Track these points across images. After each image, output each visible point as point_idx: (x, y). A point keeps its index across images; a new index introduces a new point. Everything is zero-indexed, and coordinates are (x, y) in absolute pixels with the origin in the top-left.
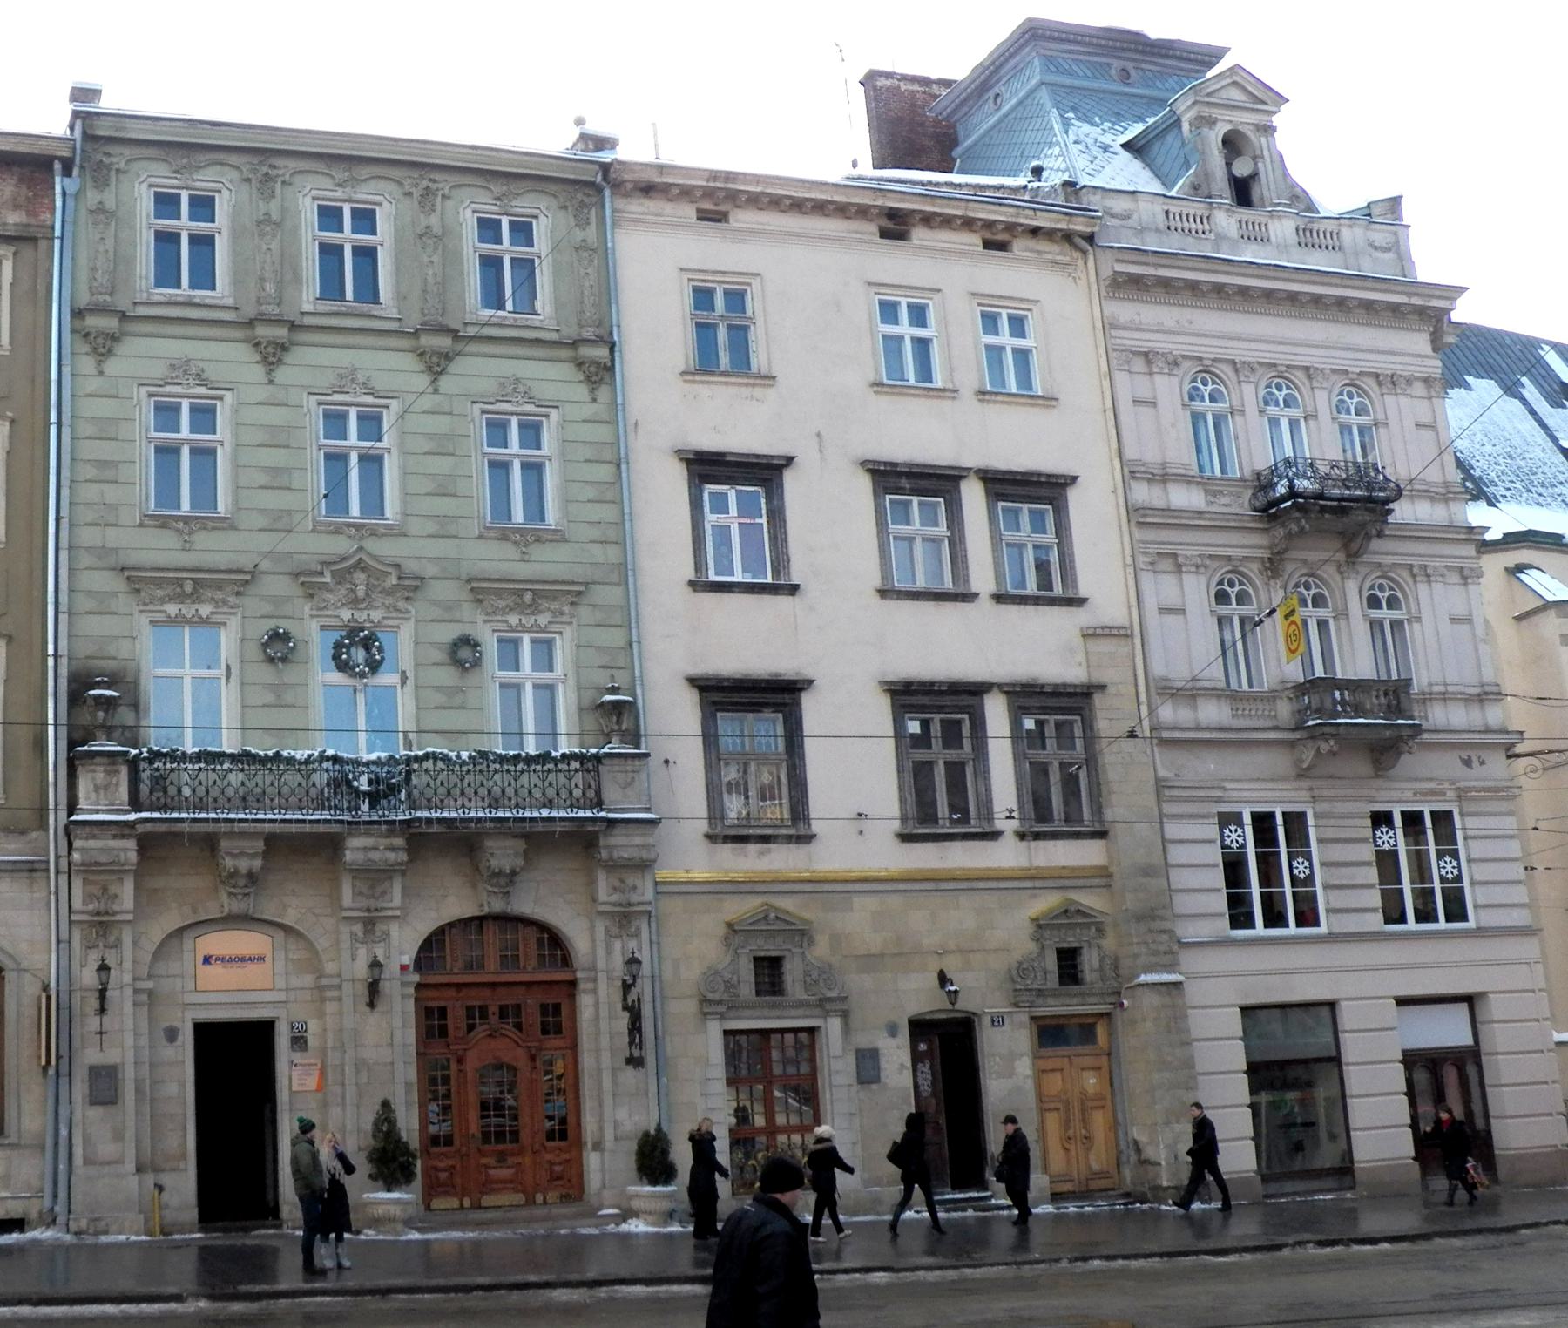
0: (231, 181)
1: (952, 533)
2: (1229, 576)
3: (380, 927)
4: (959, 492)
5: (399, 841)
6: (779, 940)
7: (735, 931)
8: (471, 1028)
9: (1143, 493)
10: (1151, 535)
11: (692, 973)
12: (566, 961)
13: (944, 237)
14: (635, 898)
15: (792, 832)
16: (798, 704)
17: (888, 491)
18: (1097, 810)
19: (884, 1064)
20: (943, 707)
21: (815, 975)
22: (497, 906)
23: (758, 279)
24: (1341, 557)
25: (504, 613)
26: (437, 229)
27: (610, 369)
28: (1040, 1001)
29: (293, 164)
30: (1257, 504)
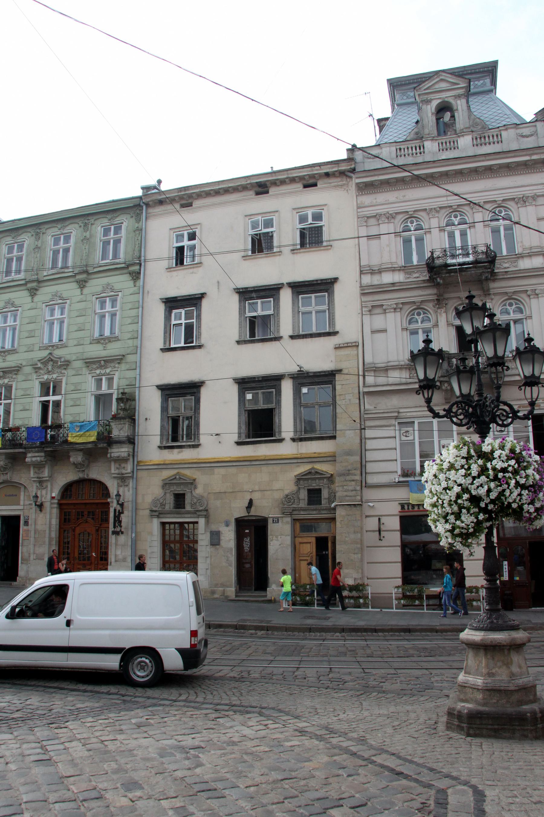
0: (28, 237)
2: (417, 311)
3: (44, 485)
4: (279, 294)
5: (42, 454)
8: (78, 519)
10: (370, 298)
11: (149, 499)
14: (124, 471)
16: (199, 392)
17: (246, 299)
19: (222, 538)
21: (195, 500)
22: (81, 475)
23: (200, 225)
25: (96, 370)
26: (88, 237)
28: (295, 512)
29: (47, 226)
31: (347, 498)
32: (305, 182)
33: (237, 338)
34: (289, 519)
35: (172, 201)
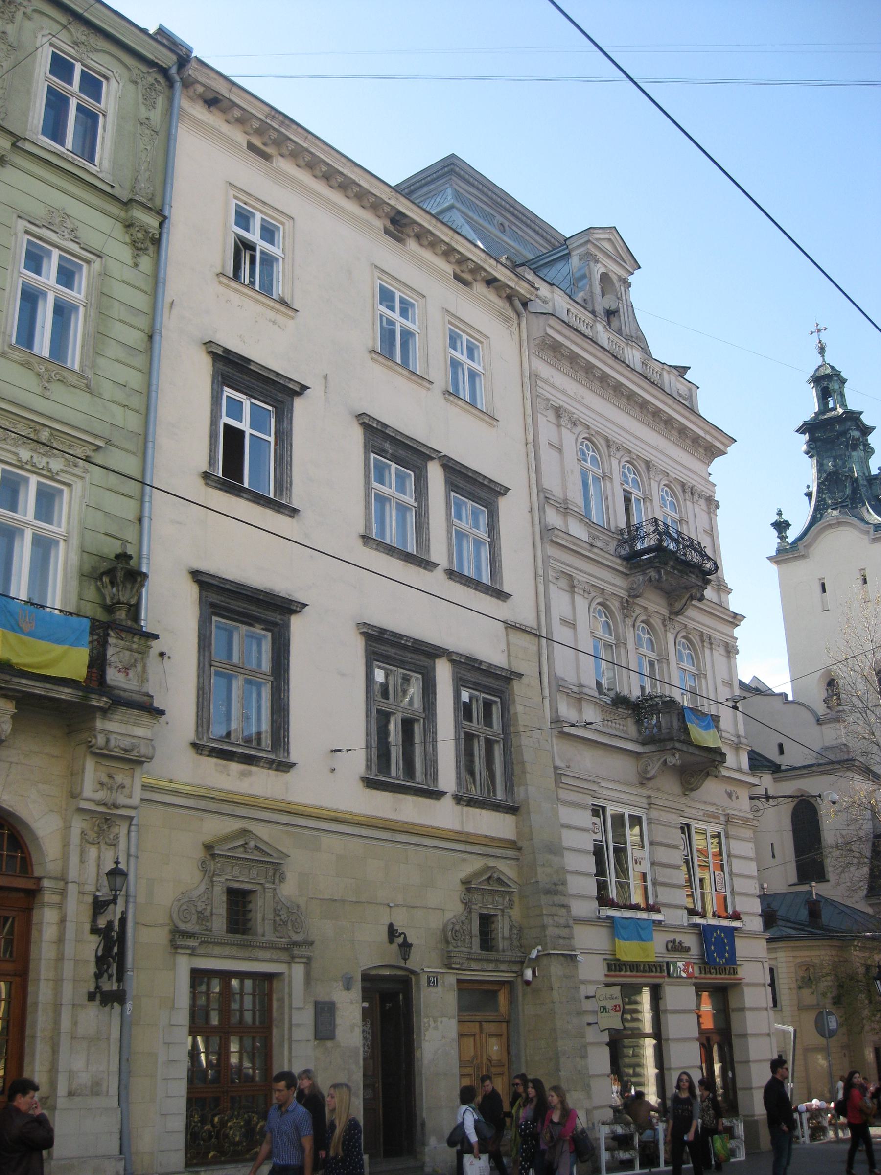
1: (418, 506)
4: (427, 472)
6: (254, 872)
7: (213, 856)
9: (553, 518)
12: (25, 865)
13: (427, 255)
14: (122, 800)
15: (273, 757)
16: (286, 626)
18: (509, 788)
19: (338, 1021)
20: (403, 662)
23: (291, 221)
24: (665, 612)
27: (157, 242)
30: (623, 553)
31: (561, 941)
32: (458, 271)
33: (362, 532)
34: (451, 979)
35: (243, 120)
